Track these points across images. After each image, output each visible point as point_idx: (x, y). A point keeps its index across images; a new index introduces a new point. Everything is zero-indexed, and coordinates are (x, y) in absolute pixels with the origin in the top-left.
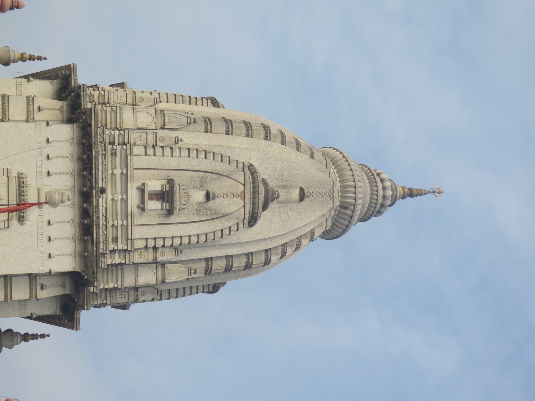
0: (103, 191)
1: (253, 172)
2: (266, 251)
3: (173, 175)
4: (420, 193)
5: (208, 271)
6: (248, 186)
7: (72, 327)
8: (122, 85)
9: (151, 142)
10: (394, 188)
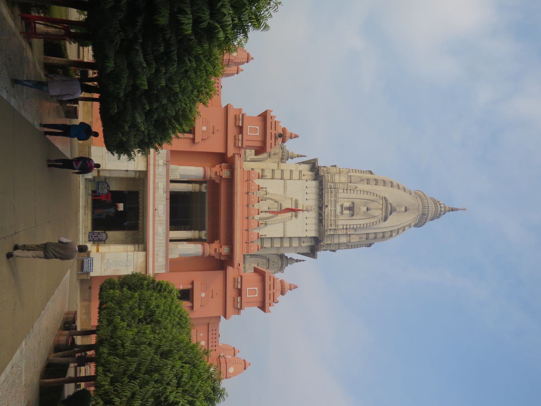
0: (327, 206)
1: (386, 199)
2: (391, 231)
4: (456, 210)
5: (367, 238)
6: (384, 205)
7: (314, 258)
8: (335, 166)
9: (346, 188)
10: (445, 207)
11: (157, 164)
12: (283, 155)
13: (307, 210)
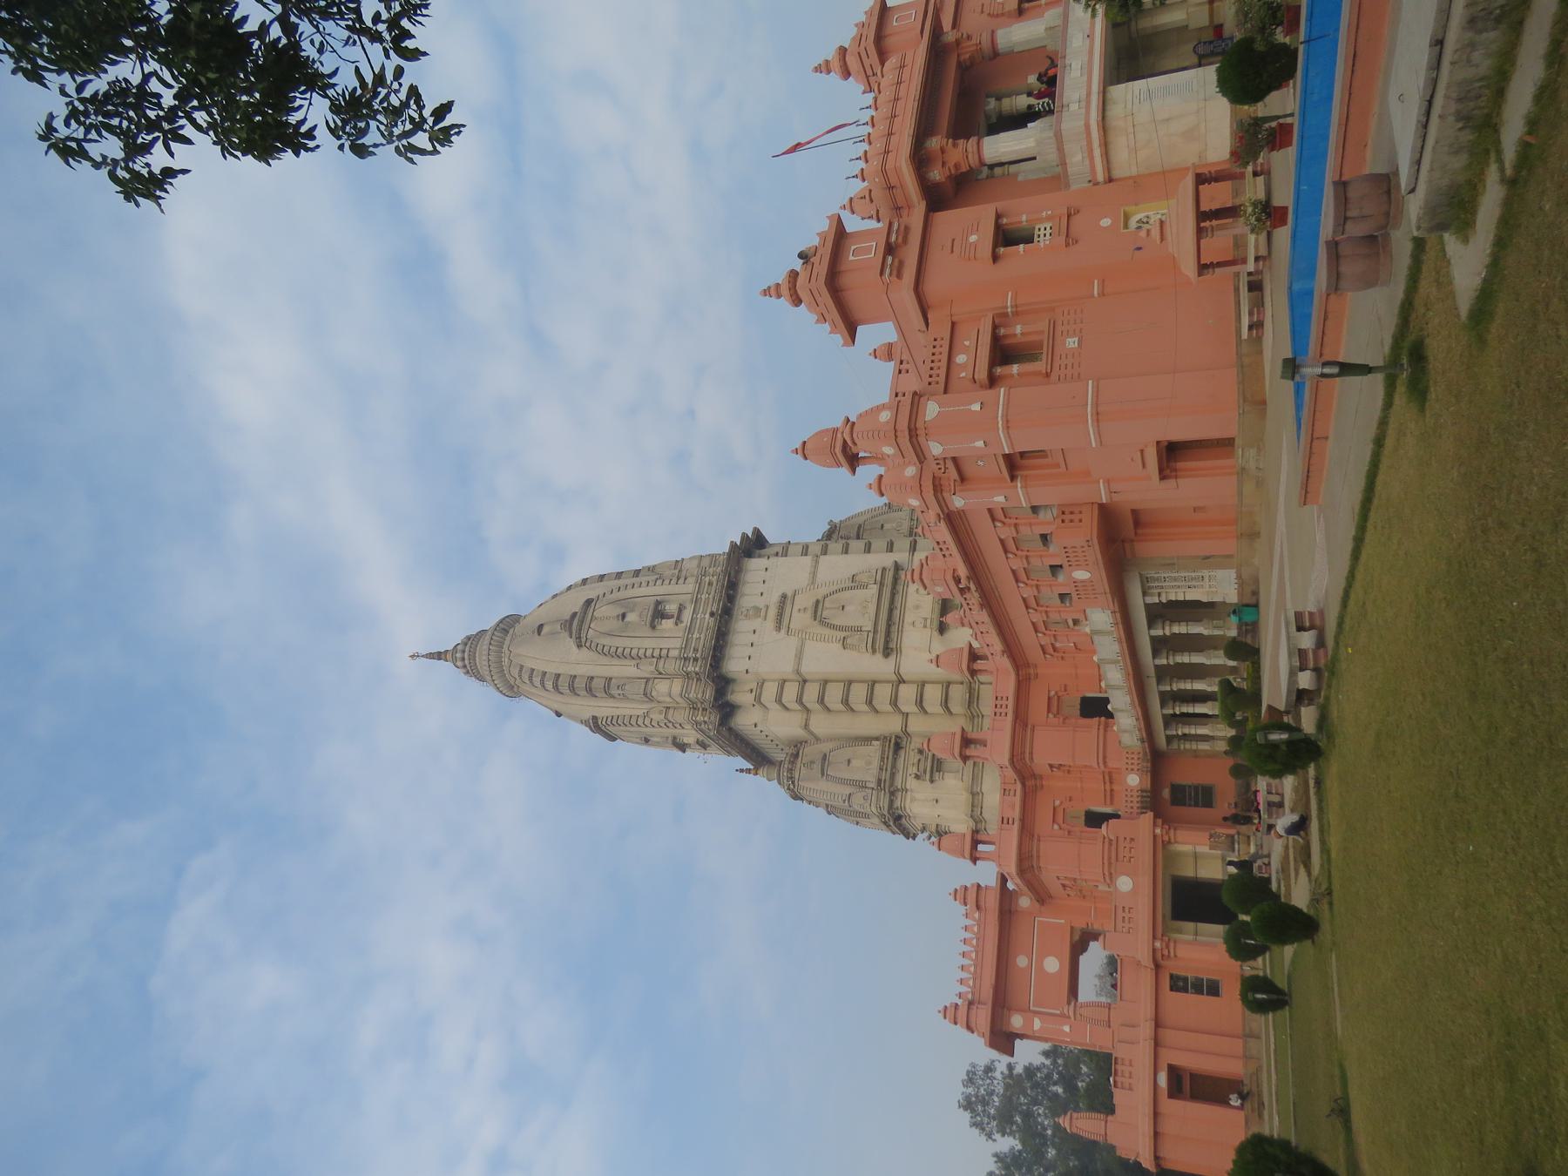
0: (712, 614)
3: (649, 633)
4: (430, 656)
11: (1083, 104)
12: (793, 763)
13: (757, 610)
